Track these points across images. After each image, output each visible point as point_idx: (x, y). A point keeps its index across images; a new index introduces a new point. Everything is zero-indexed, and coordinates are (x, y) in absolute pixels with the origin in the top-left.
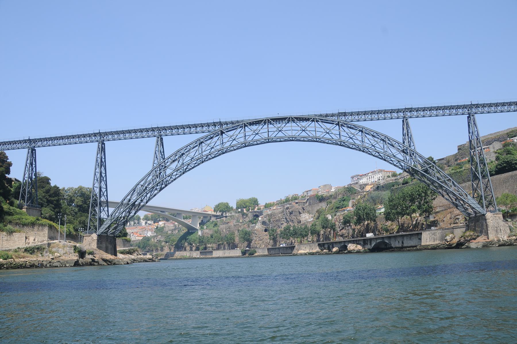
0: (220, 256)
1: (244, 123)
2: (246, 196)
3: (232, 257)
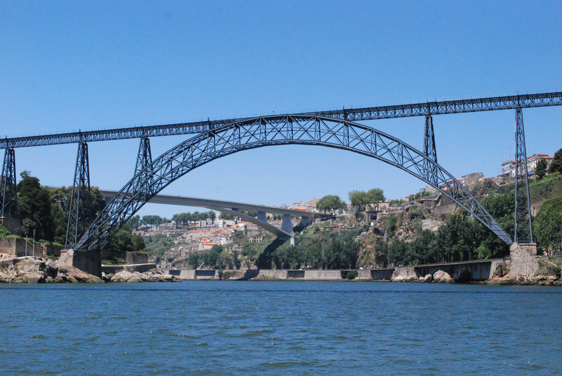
0: (314, 278)
1: (235, 124)
3: (328, 281)
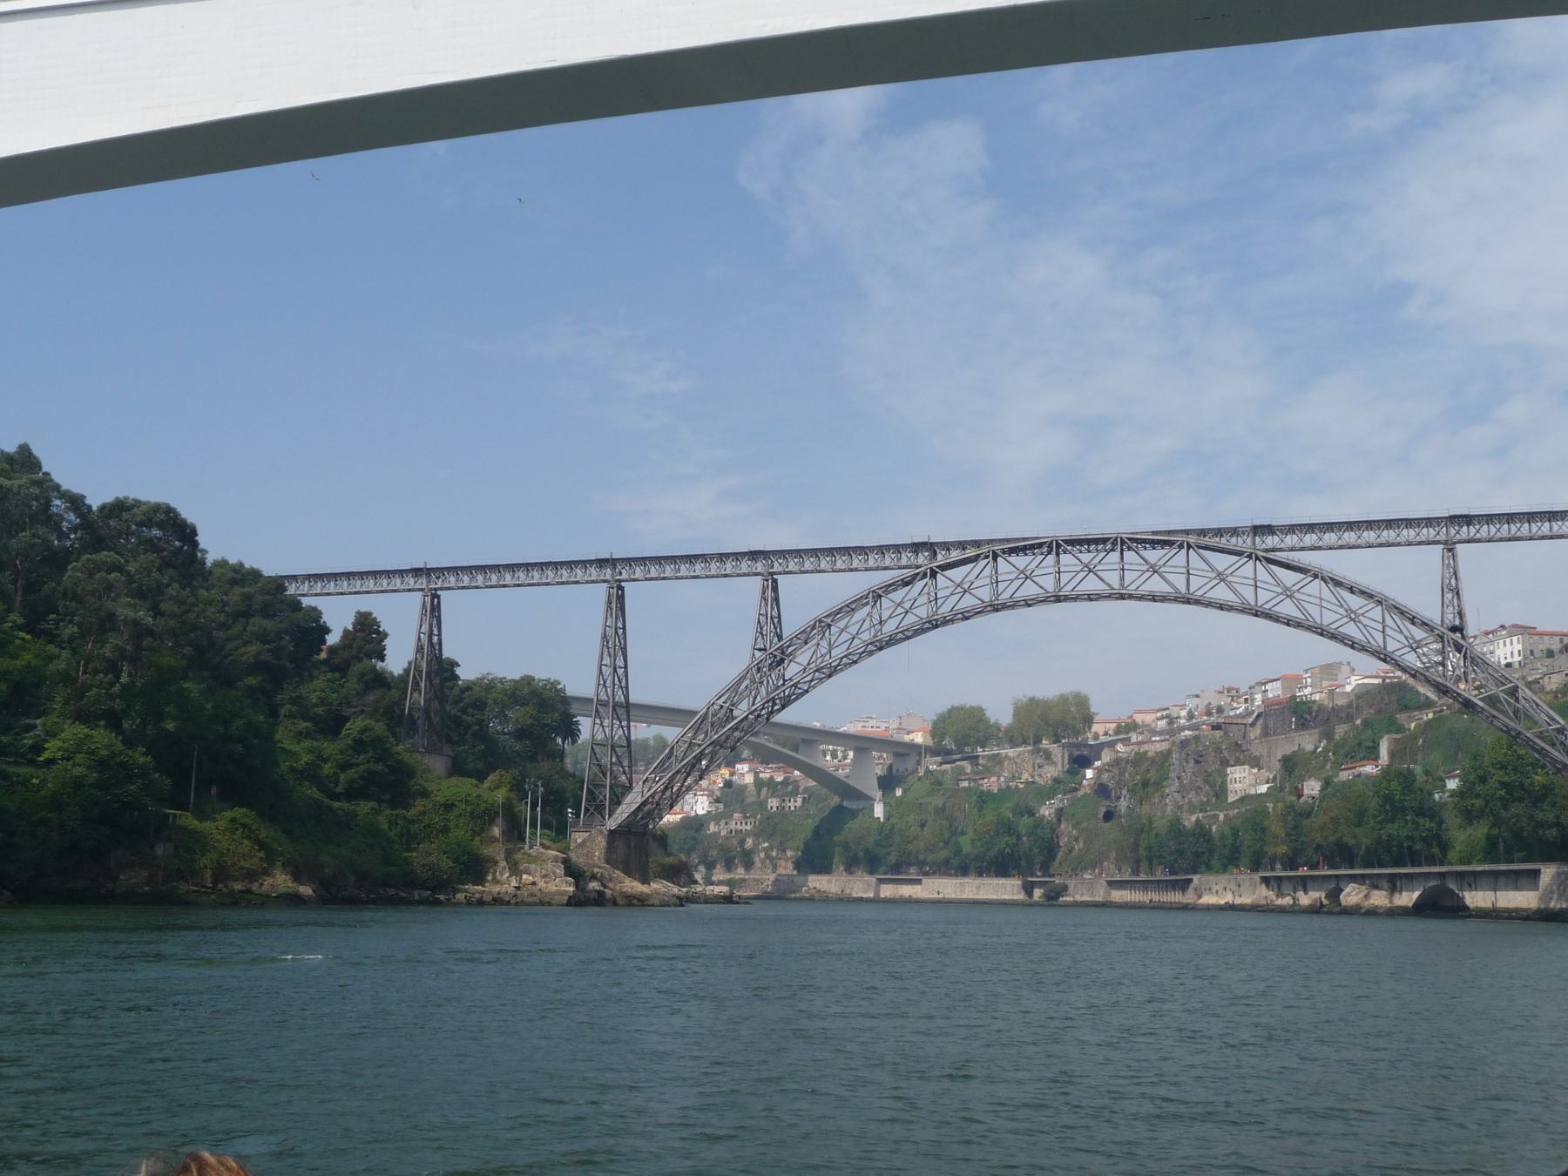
0: (947, 896)
2: (1048, 690)
